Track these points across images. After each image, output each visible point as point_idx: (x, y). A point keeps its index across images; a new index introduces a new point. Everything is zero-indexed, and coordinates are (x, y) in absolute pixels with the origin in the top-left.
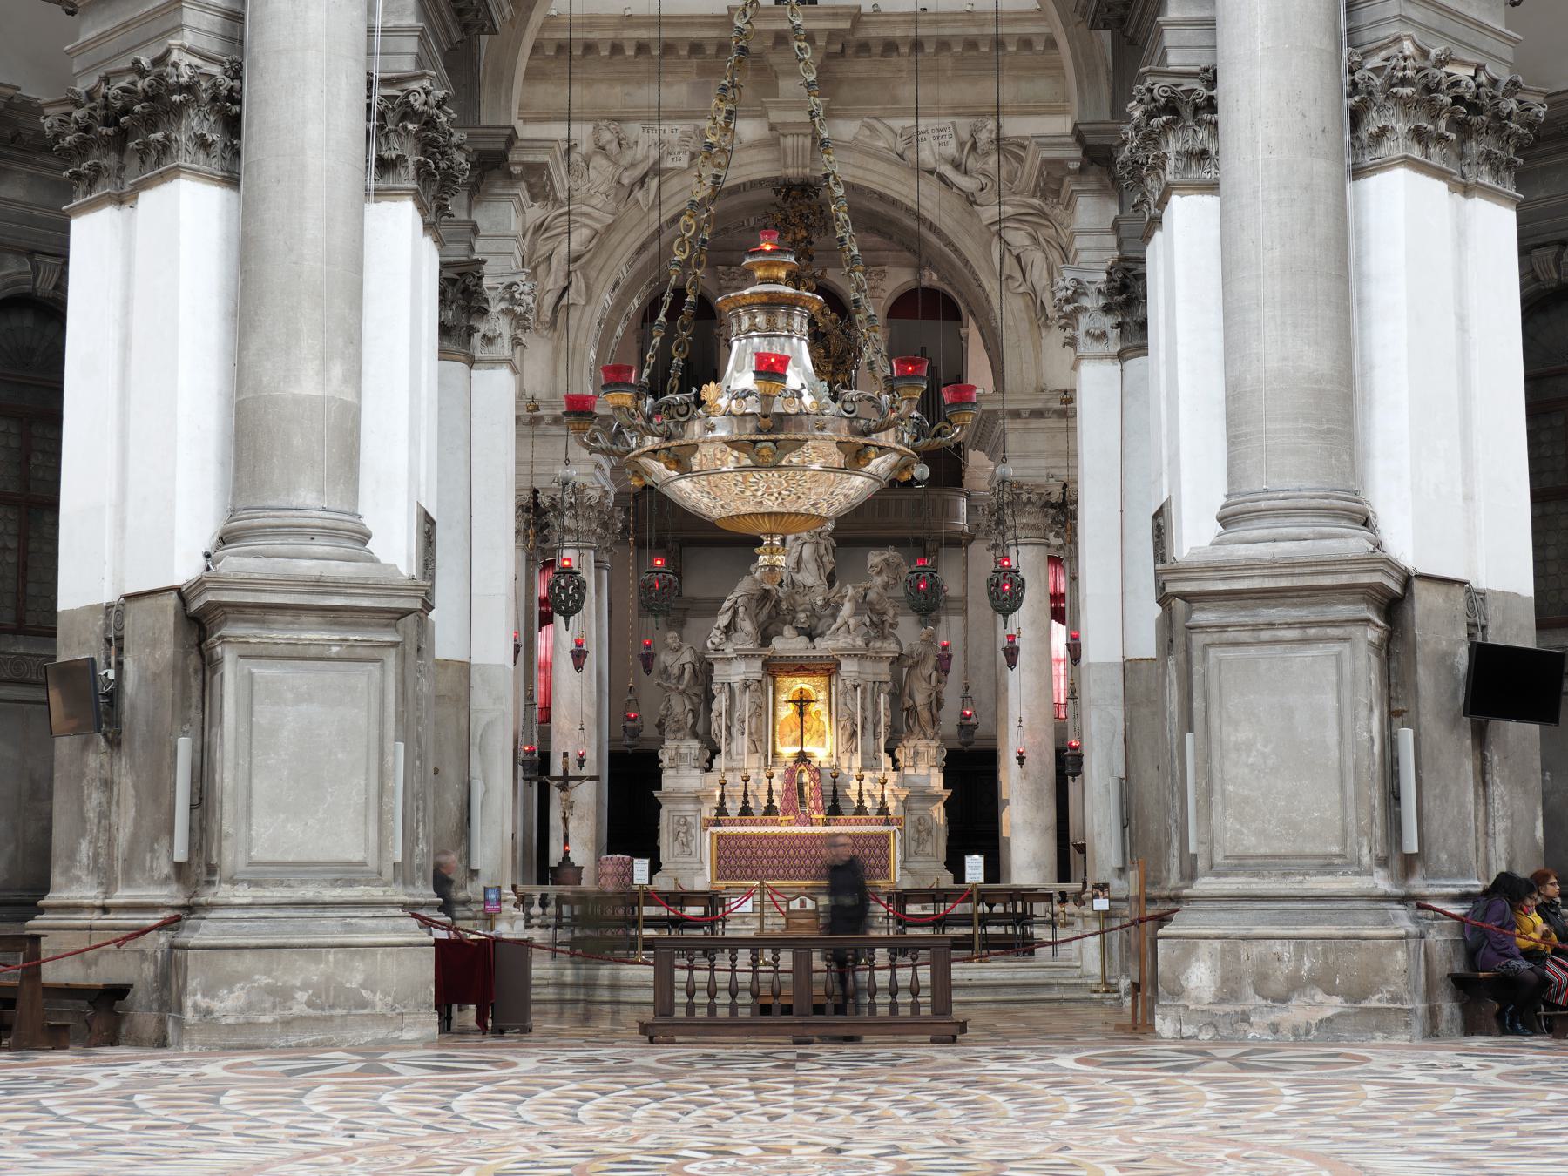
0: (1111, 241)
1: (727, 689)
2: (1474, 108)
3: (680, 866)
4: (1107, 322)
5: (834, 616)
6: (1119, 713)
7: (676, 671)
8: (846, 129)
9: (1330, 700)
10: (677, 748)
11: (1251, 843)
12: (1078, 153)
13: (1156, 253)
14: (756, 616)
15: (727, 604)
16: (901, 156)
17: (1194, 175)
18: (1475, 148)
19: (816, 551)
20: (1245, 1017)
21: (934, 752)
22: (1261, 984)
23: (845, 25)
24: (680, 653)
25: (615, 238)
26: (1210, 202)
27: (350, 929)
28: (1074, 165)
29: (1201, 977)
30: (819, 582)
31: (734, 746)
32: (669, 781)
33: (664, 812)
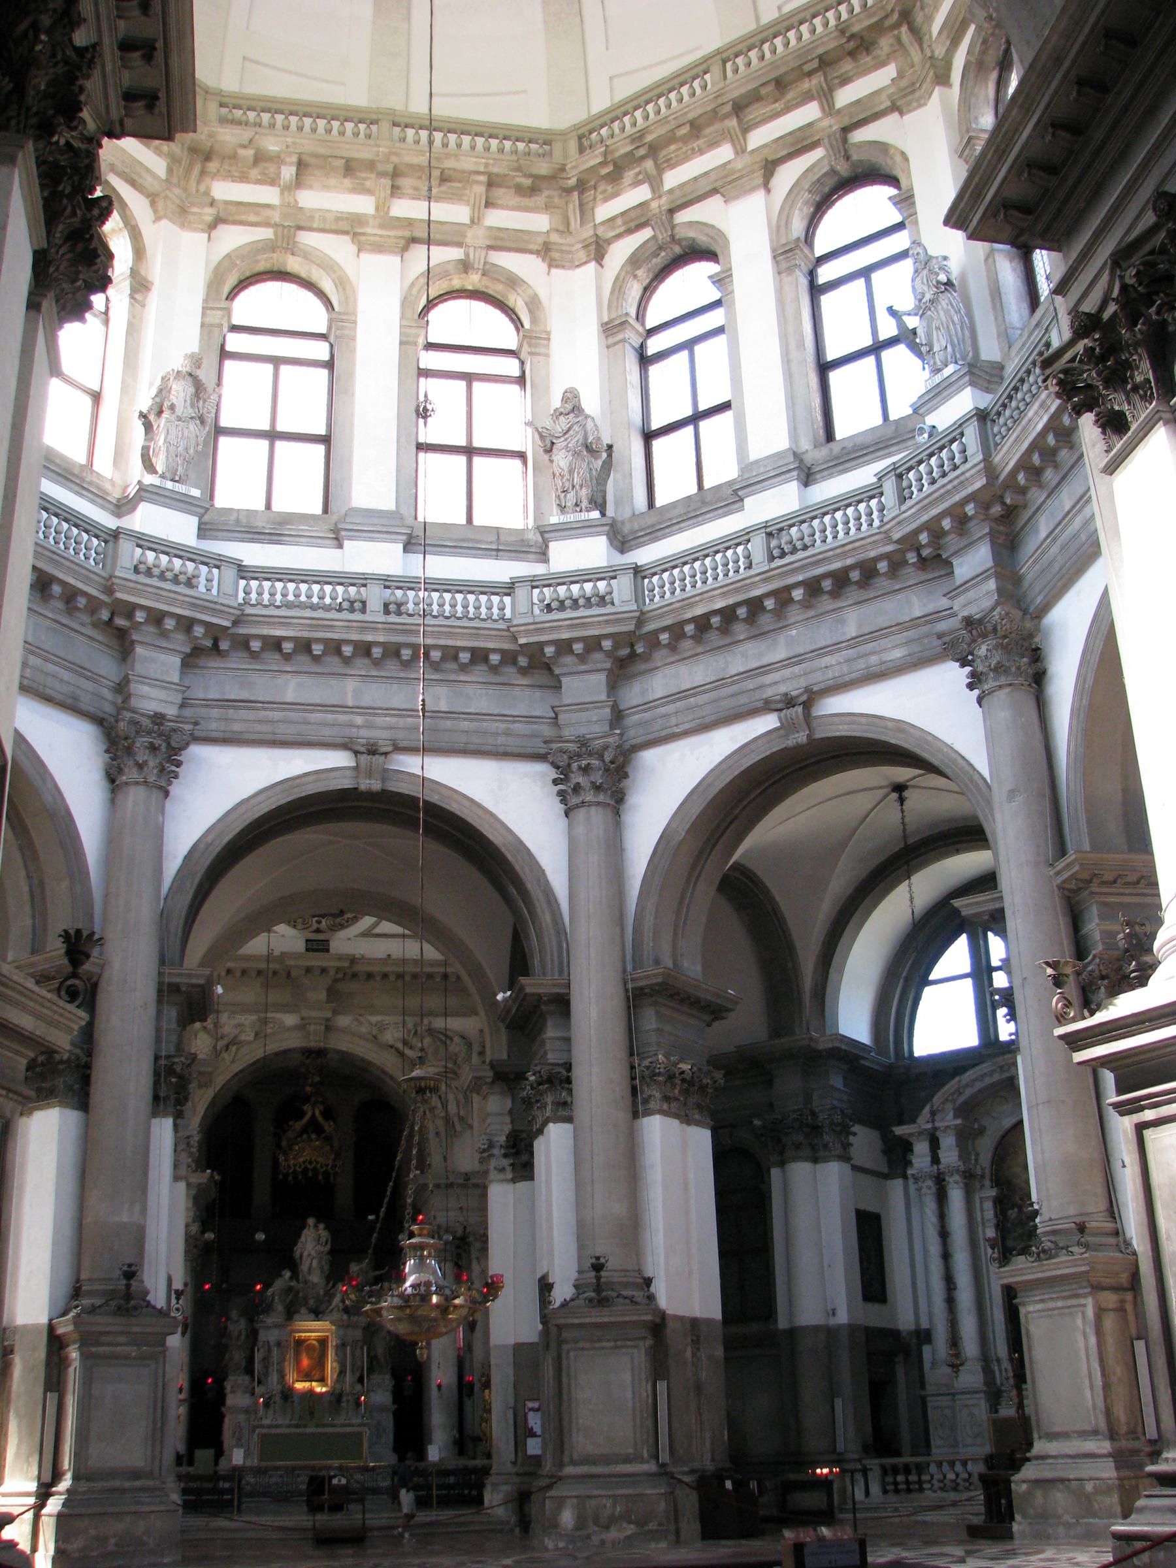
0: (508, 1119)
2: (691, 1083)
4: (506, 1162)
5: (330, 1302)
6: (511, 1372)
7: (236, 1333)
8: (344, 1021)
9: (627, 1377)
11: (591, 1449)
12: (490, 1074)
13: (539, 1145)
16: (375, 1037)
17: (561, 1113)
18: (692, 1101)
19: (320, 1262)
20: (588, 1537)
21: (387, 1382)
22: (596, 1522)
23: (346, 964)
26: (567, 1127)
27: (137, 1503)
28: (489, 1080)
29: (567, 1518)
32: (231, 1400)
33: (227, 1420)
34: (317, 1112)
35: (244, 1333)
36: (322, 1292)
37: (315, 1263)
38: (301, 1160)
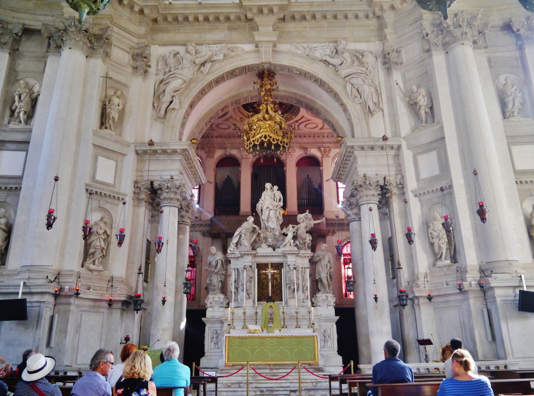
1: (236, 271)
3: (213, 354)
5: (283, 240)
7: (214, 264)
10: (214, 298)
14: (250, 240)
15: (236, 233)
24: (215, 256)
25: (192, 85)
30: (277, 227)
31: (239, 297)
33: (207, 328)
34: (269, 108)
35: (220, 262)
36: (277, 233)
37: (272, 213)
38: (258, 137)
